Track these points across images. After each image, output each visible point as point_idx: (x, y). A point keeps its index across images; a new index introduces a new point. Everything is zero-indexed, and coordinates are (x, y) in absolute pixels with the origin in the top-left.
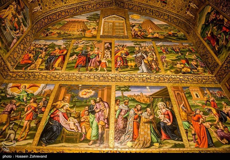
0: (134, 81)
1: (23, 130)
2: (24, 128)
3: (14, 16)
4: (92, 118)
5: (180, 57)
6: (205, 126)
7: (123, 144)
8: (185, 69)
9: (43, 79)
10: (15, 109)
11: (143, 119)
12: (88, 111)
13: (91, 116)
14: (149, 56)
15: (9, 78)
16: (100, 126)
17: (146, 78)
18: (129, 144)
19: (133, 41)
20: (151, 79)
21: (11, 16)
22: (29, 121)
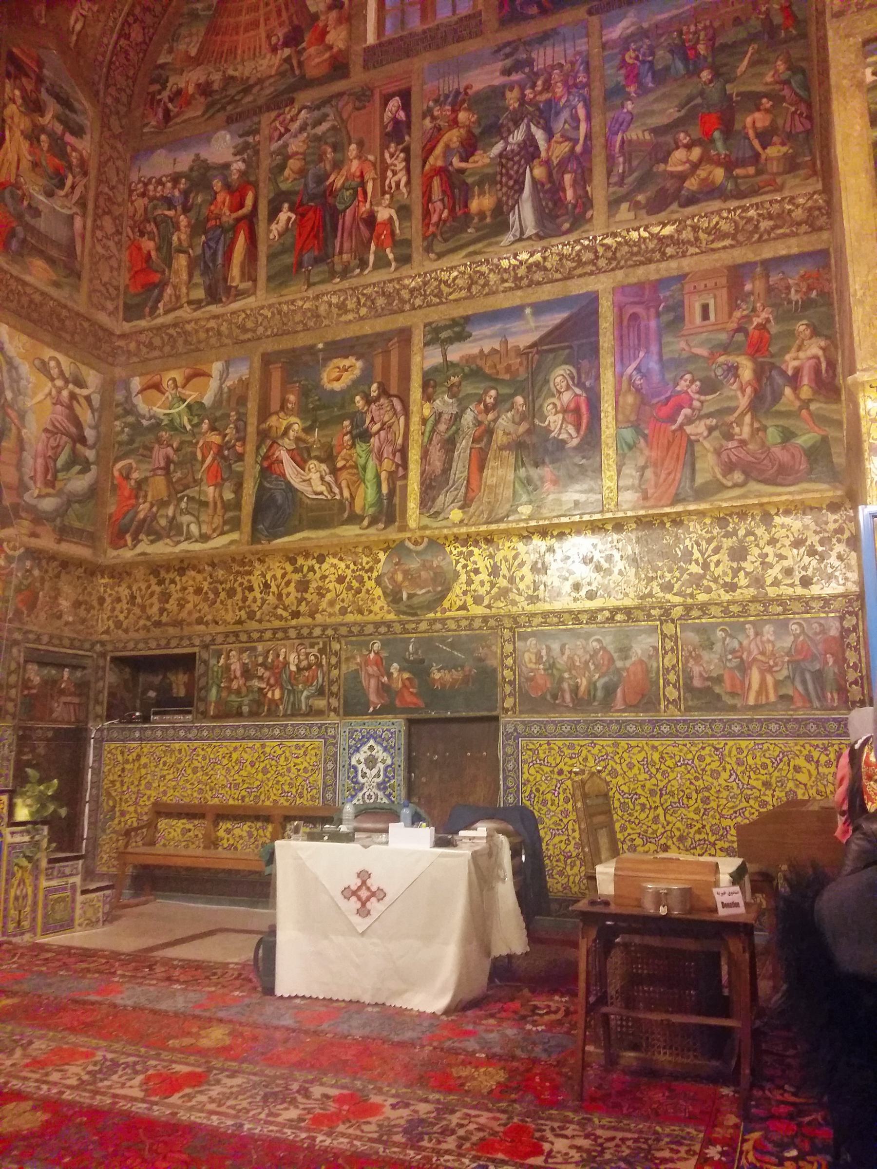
0: (487, 290)
1: (210, 511)
2: (211, 505)
3: (32, 136)
4: (363, 455)
5: (699, 100)
6: (688, 436)
7: (441, 517)
8: (702, 173)
9: (213, 341)
10: (175, 458)
11: (499, 438)
12: (350, 432)
13: (361, 448)
14: (557, 136)
15: (123, 359)
16: (384, 475)
17: (529, 268)
18: (456, 515)
19: (499, 50)
20: (545, 269)
21: (25, 146)
22: (215, 486)
